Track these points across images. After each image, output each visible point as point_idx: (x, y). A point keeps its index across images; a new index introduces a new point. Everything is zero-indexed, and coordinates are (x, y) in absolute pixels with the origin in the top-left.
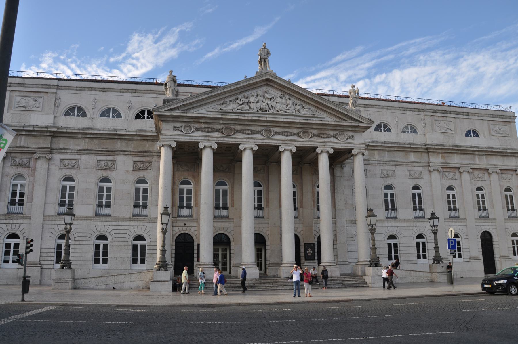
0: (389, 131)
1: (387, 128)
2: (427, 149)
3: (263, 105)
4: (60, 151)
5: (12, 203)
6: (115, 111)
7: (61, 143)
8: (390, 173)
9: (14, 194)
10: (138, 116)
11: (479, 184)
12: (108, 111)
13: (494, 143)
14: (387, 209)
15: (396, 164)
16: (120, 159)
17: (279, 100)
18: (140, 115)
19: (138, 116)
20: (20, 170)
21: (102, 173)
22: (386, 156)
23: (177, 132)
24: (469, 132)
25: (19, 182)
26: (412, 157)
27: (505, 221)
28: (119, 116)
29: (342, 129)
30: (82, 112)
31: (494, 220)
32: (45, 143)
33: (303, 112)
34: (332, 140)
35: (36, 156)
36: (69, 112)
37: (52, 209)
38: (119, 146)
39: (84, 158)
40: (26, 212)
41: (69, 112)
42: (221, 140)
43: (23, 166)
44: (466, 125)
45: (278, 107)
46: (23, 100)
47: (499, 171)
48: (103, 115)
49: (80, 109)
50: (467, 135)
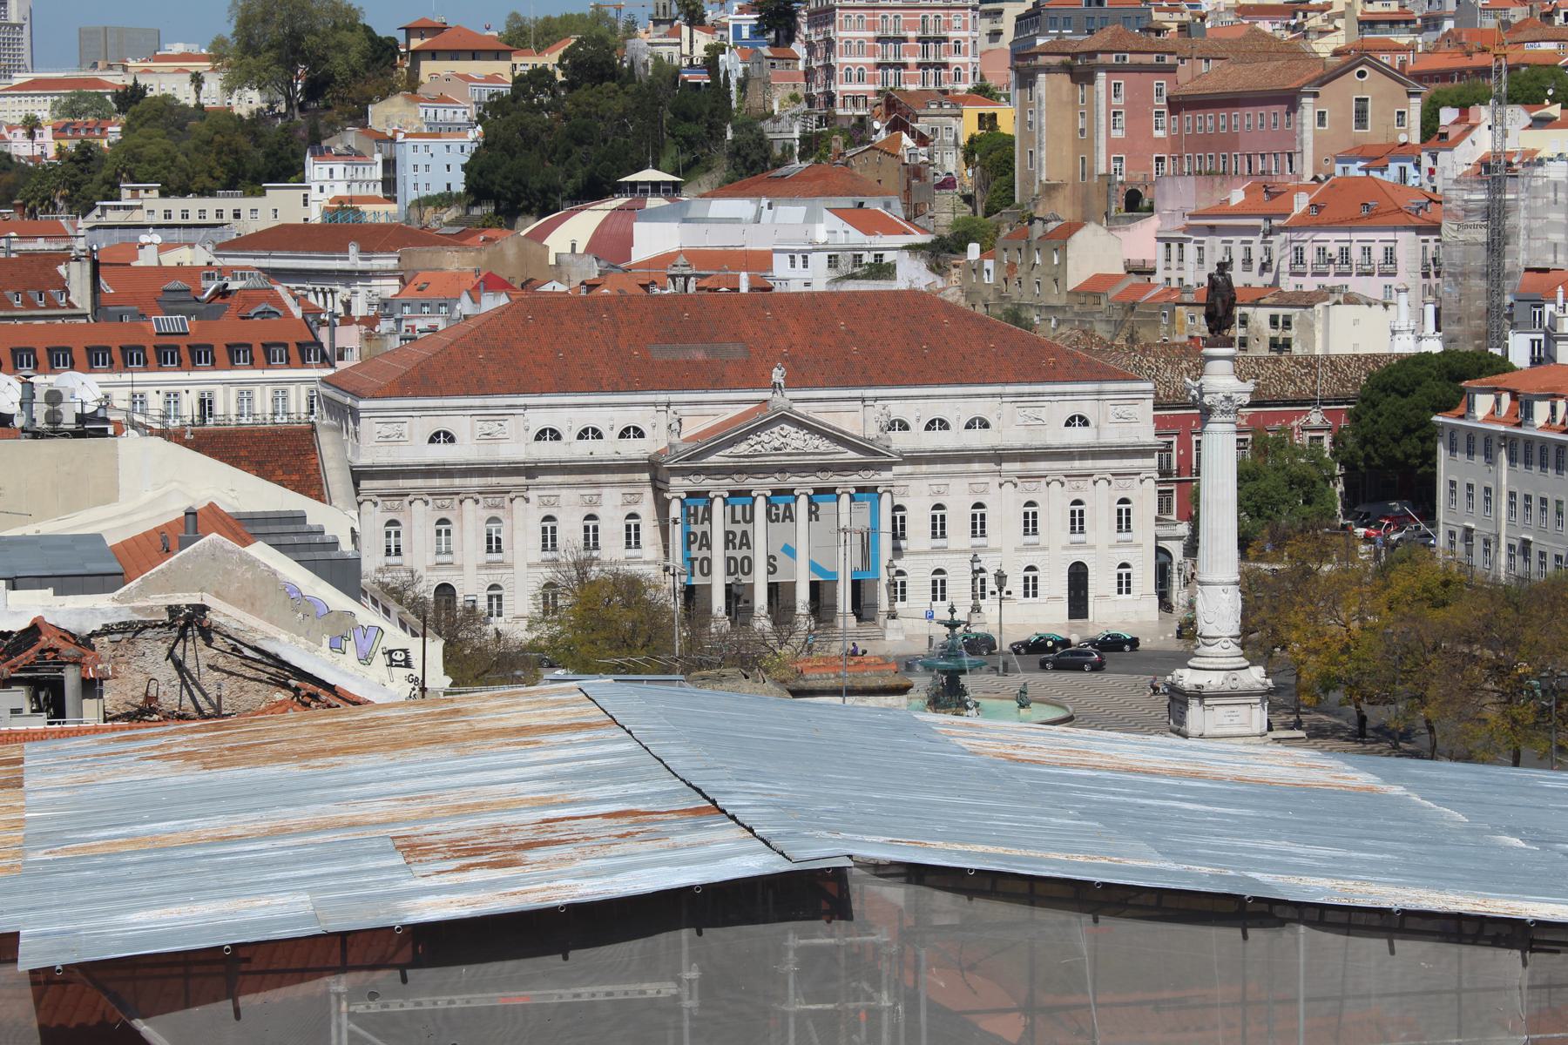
0: (947, 427)
1: (944, 425)
2: (998, 456)
3: (777, 444)
4: (538, 486)
5: (489, 550)
6: (595, 430)
7: (541, 479)
8: (942, 489)
9: (489, 540)
10: (622, 436)
11: (1077, 496)
12: (586, 431)
13: (1113, 435)
14: (934, 535)
15: (952, 475)
16: (606, 491)
17: (794, 435)
18: (624, 434)
19: (622, 436)
20: (494, 513)
21: (587, 511)
22: (938, 468)
23: (686, 482)
24: (1073, 418)
25: (494, 527)
26: (976, 467)
27: (1111, 547)
28: (600, 436)
29: (866, 467)
30: (556, 435)
31: (1093, 547)
32: (521, 480)
33: (822, 449)
34: (855, 477)
35: (512, 495)
36: (540, 436)
37: (537, 555)
38: (603, 478)
39: (564, 493)
40: (508, 560)
41: (540, 436)
42: (732, 488)
43: (496, 507)
44: (1070, 409)
45: (795, 444)
46: (486, 425)
47: (1110, 477)
48: (580, 437)
49: (552, 431)
50: (1068, 424)
